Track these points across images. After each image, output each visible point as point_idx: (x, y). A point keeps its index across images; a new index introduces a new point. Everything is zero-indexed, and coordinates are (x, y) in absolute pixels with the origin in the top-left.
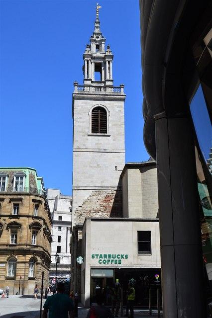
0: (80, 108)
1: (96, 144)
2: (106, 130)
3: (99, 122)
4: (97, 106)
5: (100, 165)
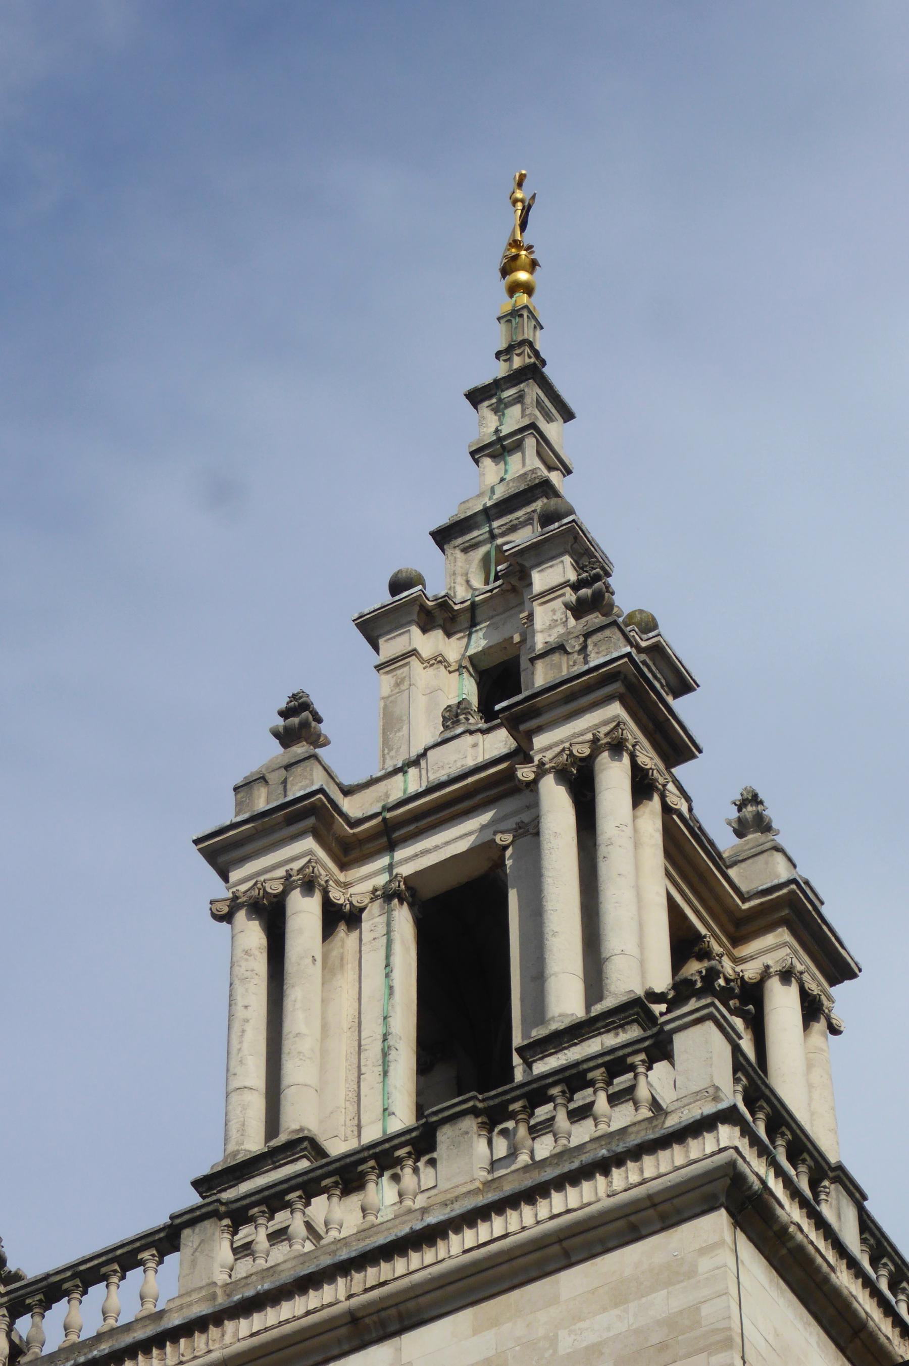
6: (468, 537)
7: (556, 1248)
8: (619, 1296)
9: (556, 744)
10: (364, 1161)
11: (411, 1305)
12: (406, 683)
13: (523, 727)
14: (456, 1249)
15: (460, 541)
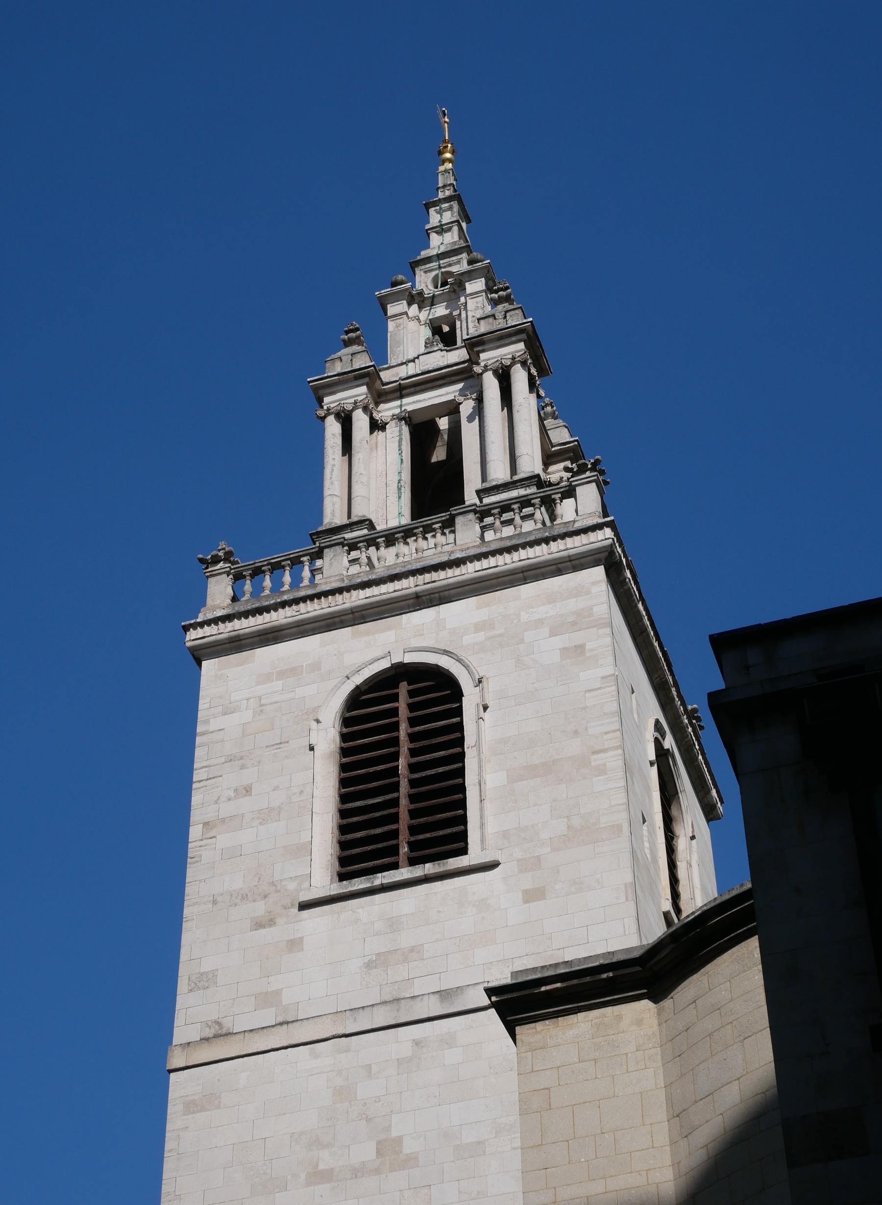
0: (246, 716)
1: (378, 962)
2: (463, 836)
3: (403, 785)
4: (385, 664)
5: (409, 1147)
6: (428, 266)
7: (521, 575)
8: (551, 599)
9: (492, 358)
10: (417, 528)
12: (402, 327)
13: (476, 349)
14: (470, 570)
15: (423, 267)
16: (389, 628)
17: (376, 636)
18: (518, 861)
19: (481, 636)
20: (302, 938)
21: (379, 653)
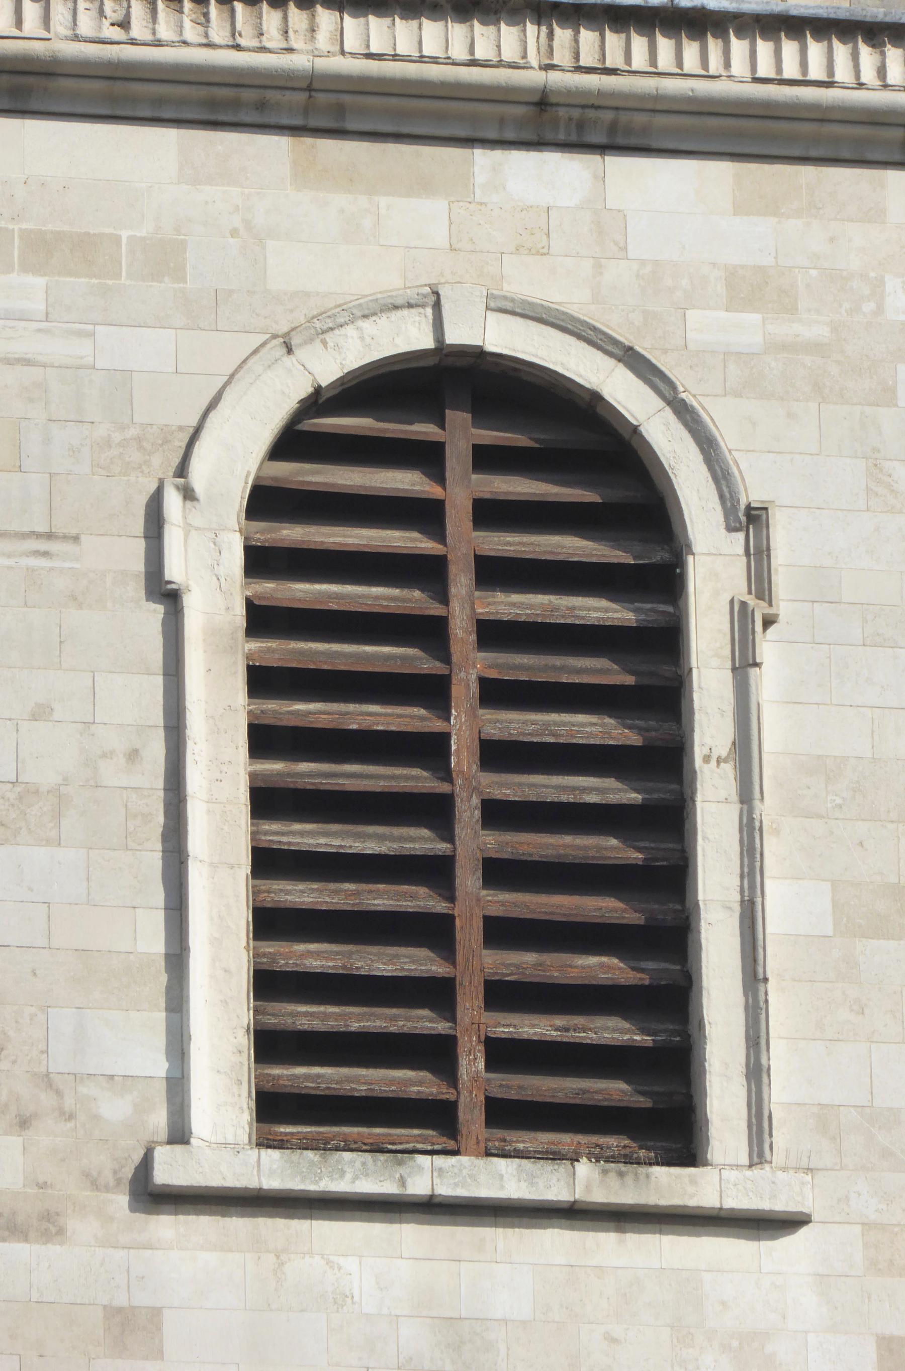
4: (411, 335)
11: (640, 119)
16: (424, 186)
17: (383, 201)
18: (868, 1226)
19: (748, 329)
20: (155, 1314)
21: (389, 280)
